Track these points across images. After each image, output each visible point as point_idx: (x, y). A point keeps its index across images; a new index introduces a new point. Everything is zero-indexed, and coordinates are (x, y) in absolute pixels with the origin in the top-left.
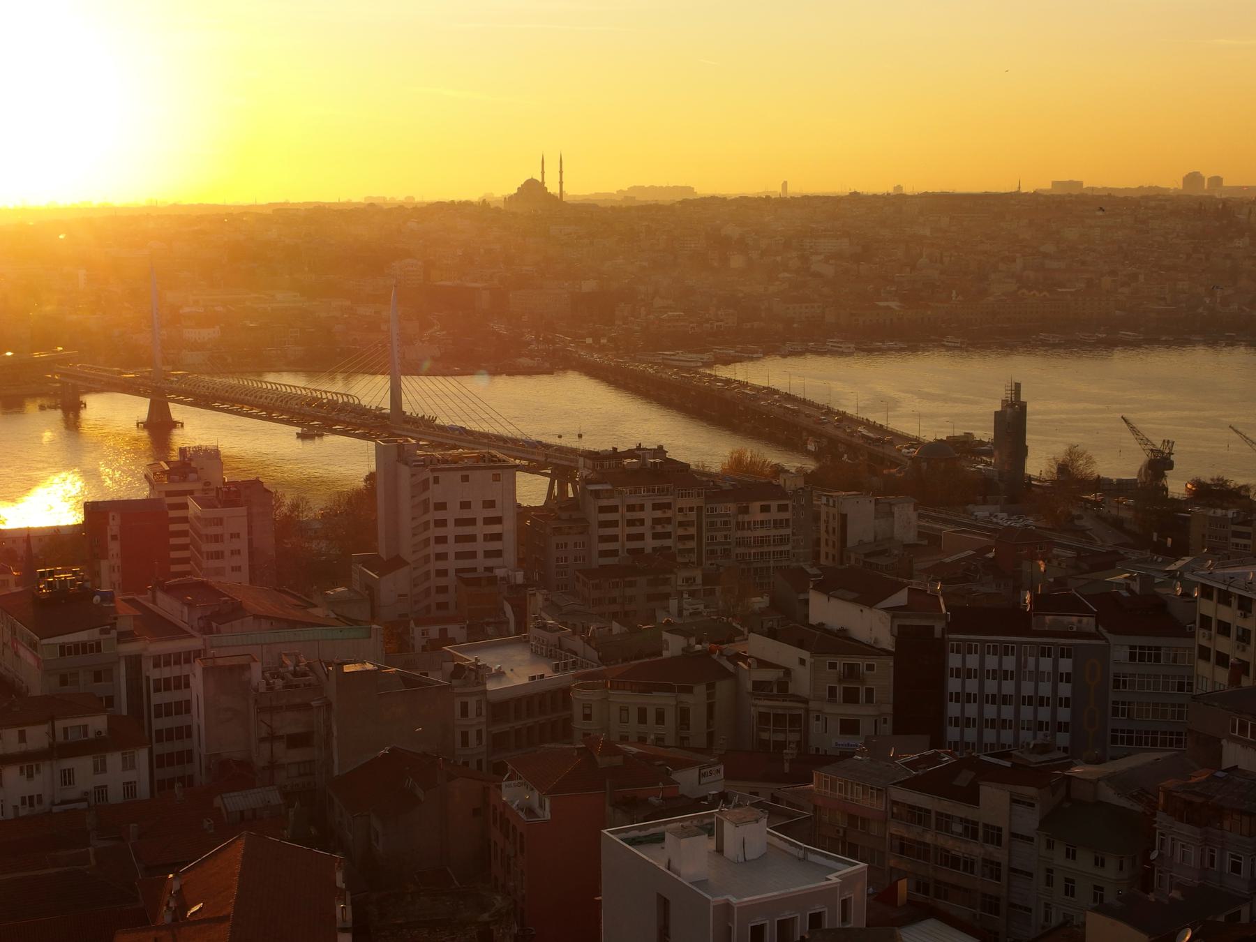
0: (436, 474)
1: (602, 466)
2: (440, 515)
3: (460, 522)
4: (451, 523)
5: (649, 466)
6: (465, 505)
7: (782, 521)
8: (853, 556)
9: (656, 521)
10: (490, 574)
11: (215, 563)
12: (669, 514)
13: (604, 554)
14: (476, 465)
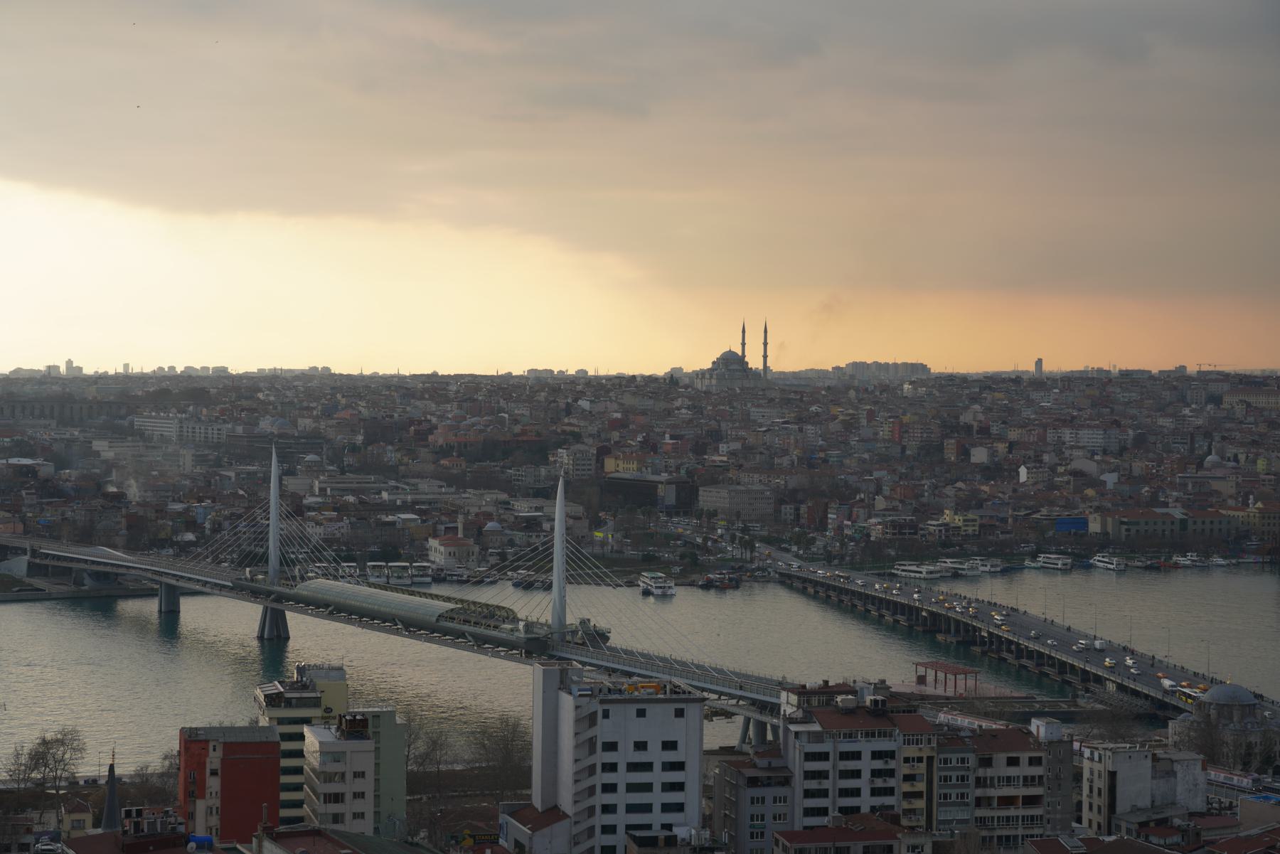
0: (606, 707)
1: (808, 702)
2: (609, 757)
3: (633, 767)
4: (622, 767)
5: (868, 703)
6: (641, 746)
7: (1033, 778)
8: (1124, 825)
9: (876, 773)
10: (668, 833)
11: (334, 808)
12: (892, 764)
13: (809, 812)
14: (654, 697)
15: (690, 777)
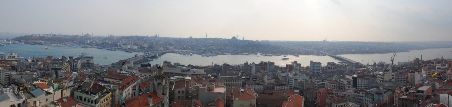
3: (317, 68)
6: (317, 67)
15: (321, 69)
